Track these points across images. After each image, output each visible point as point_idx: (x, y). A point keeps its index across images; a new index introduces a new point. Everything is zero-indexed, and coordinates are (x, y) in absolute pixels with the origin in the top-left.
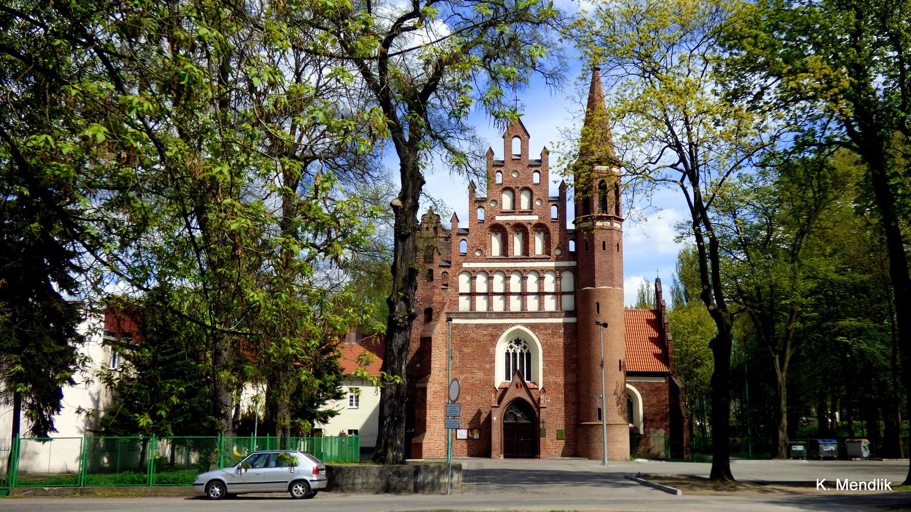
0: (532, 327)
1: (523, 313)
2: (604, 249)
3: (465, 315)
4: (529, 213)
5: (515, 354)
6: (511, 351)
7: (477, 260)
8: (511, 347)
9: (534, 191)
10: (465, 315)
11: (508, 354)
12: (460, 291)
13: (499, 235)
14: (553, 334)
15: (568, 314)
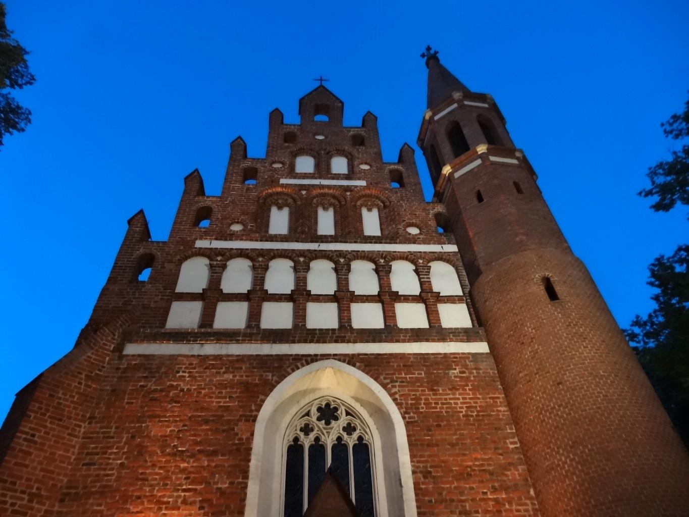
0: (369, 364)
1: (345, 331)
2: (519, 191)
3: (180, 336)
4: (348, 177)
5: (318, 449)
6: (307, 442)
7: (232, 236)
8: (307, 429)
9: (355, 153)
10: (180, 336)
11: (294, 450)
12: (180, 288)
13: (286, 211)
14: (433, 384)
15: (466, 335)
